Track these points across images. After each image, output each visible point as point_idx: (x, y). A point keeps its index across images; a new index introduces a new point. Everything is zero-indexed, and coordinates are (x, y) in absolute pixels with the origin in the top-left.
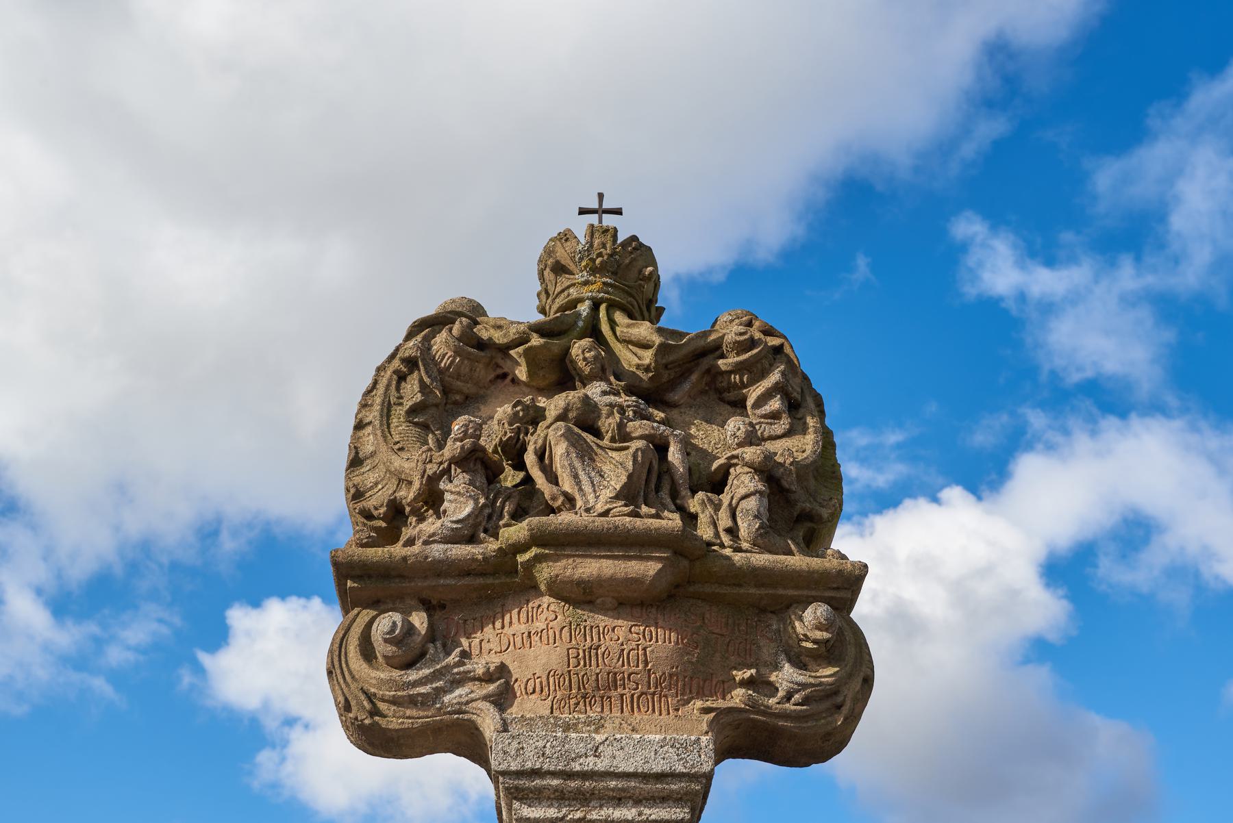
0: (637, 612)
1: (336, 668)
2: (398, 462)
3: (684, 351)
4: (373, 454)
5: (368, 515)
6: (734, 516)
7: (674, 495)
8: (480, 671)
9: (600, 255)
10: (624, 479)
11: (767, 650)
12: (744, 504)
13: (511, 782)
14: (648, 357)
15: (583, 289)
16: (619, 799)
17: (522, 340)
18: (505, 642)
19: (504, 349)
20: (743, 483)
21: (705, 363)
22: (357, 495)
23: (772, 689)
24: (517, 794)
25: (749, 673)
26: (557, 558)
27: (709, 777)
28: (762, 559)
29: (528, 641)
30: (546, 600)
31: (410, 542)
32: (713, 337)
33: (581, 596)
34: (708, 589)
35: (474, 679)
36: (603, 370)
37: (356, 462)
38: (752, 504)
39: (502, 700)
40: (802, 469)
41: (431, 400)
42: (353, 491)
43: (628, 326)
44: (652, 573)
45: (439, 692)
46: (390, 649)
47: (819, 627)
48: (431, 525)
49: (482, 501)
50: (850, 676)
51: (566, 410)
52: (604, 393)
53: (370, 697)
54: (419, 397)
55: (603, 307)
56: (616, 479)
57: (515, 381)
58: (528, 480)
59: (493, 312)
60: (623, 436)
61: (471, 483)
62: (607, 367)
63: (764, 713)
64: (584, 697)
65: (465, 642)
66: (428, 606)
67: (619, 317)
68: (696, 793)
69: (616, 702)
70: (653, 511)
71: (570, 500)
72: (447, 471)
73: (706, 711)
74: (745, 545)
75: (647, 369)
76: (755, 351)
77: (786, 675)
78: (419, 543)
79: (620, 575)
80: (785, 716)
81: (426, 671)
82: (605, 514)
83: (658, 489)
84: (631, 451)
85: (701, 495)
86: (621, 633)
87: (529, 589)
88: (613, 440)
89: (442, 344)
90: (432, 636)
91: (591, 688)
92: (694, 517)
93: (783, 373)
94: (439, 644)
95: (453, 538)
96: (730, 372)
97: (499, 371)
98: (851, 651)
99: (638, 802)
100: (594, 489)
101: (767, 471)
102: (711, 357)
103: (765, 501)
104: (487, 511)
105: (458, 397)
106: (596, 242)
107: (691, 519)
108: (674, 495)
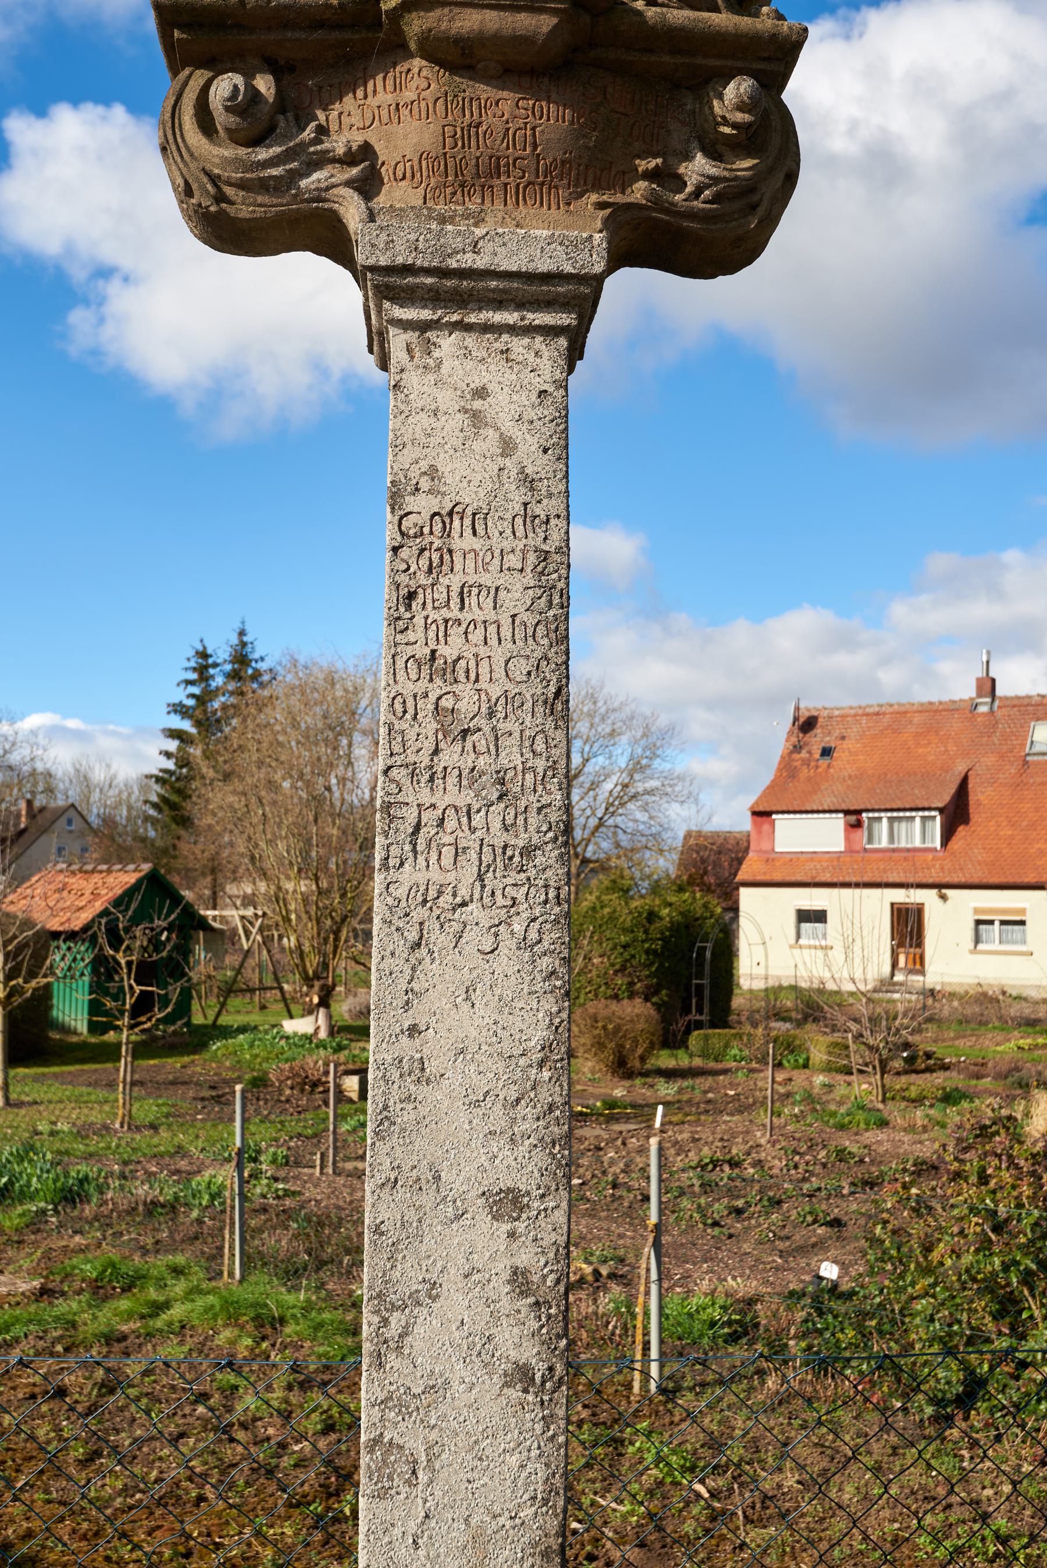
8: (340, 150)
13: (380, 279)
16: (499, 303)
18: (368, 115)
25: (653, 163)
27: (597, 282)
29: (395, 114)
30: (417, 63)
35: (335, 160)
39: (368, 186)
44: (545, 29)
46: (233, 120)
47: (741, 107)
50: (771, 170)
53: (214, 179)
63: (667, 212)
64: (462, 186)
65: (321, 115)
68: (585, 297)
69: (498, 192)
73: (601, 206)
77: (698, 167)
79: (507, 32)
80: (692, 215)
81: (278, 149)
86: (506, 107)
91: (470, 175)
94: (290, 116)
99: (520, 305)
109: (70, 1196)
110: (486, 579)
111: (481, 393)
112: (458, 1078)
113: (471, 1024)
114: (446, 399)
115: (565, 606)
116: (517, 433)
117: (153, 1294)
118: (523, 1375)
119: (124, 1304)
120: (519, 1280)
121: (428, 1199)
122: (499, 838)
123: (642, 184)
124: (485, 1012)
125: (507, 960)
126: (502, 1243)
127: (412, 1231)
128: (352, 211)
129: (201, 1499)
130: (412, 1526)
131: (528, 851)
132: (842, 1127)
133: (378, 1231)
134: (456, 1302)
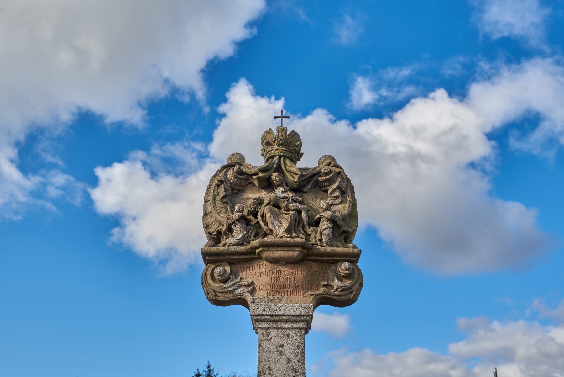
0: (292, 266)
2: (219, 218)
3: (308, 176)
4: (211, 212)
5: (210, 234)
6: (321, 235)
8: (246, 284)
9: (281, 140)
10: (287, 225)
12: (324, 232)
13: (255, 317)
14: (296, 177)
15: (276, 151)
16: (286, 321)
17: (256, 174)
18: (253, 275)
19: (251, 175)
20: (325, 224)
21: (315, 178)
22: (207, 227)
23: (332, 287)
24: (258, 321)
25: (326, 283)
26: (268, 250)
27: (312, 316)
28: (329, 249)
29: (259, 274)
30: (265, 262)
31: (224, 245)
32: (318, 169)
33: (275, 261)
34: (313, 258)
35: (244, 286)
36: (282, 183)
37: (205, 215)
38: (326, 232)
39: (252, 292)
40: (344, 218)
41: (228, 194)
42: (205, 225)
43: (290, 166)
44: (296, 255)
45: (234, 290)
46: (220, 278)
47: (346, 270)
48: (230, 240)
49: (245, 233)
50: (355, 283)
51: (270, 201)
52: (283, 192)
53: (214, 291)
54: (224, 194)
55: (282, 158)
56: (286, 225)
57: (254, 185)
58: (258, 222)
59: (247, 162)
60: (288, 210)
61: (241, 227)
63: (329, 295)
64: (276, 291)
65: (241, 275)
66: (230, 264)
67: (288, 162)
68: (308, 320)
69: (286, 293)
70: (296, 235)
71: (271, 231)
72: (234, 222)
73: (312, 295)
74: (324, 245)
75: (296, 182)
76: (331, 175)
77: (336, 283)
78: (227, 246)
79: (286, 256)
80: (336, 296)
81: (230, 284)
82: (282, 237)
83: (298, 226)
84: (290, 215)
85: (311, 228)
86: (287, 272)
87: (260, 258)
88: (284, 210)
89: (230, 174)
90: (231, 273)
91: (278, 288)
92: (309, 235)
93: (340, 182)
94: (234, 276)
95: (237, 244)
96: (323, 182)
97: (249, 181)
98: (356, 275)
99: (292, 322)
100: (279, 228)
101: (332, 220)
102: (317, 176)
103: (331, 230)
104: (247, 236)
105: (236, 191)
106: (280, 134)
107: (308, 236)
108: (304, 227)
111: (282, 346)
114: (273, 348)
116: (291, 357)
123: (322, 289)
128: (249, 298)
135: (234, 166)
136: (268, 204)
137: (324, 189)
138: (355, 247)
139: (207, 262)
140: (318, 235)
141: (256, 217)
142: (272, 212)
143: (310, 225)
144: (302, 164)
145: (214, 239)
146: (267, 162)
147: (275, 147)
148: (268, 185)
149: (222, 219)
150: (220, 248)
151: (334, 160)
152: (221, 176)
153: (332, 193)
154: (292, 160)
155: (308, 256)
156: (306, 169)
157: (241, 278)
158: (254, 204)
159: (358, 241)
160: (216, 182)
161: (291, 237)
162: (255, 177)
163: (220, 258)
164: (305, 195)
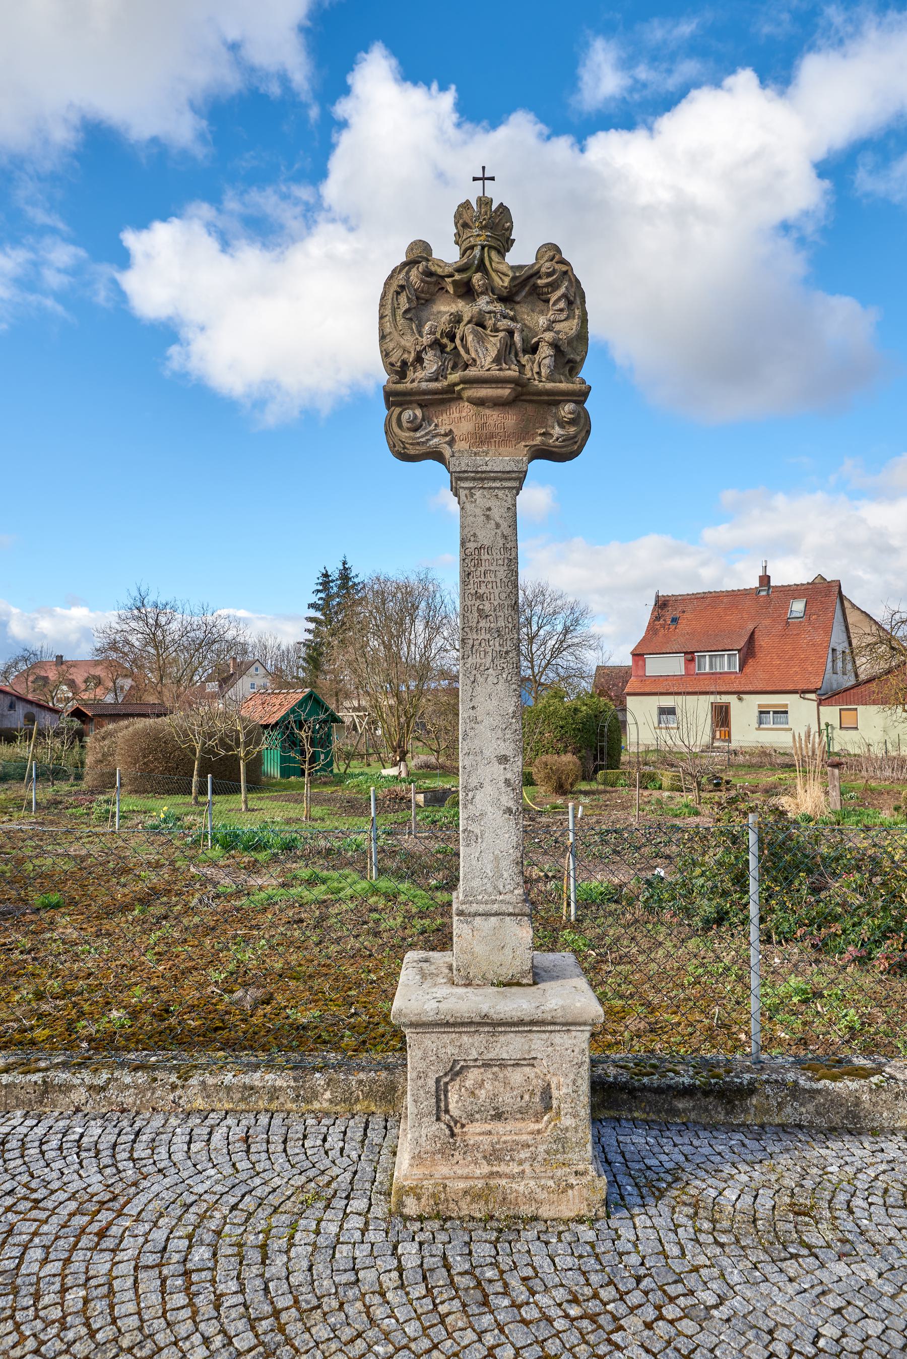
1: (388, 431)
2: (403, 343)
5: (392, 365)
7: (516, 355)
11: (550, 421)
14: (507, 281)
16: (494, 479)
17: (451, 276)
19: (443, 277)
20: (545, 351)
22: (386, 354)
24: (459, 479)
26: (470, 388)
27: (526, 472)
28: (550, 386)
29: (459, 420)
31: (413, 381)
33: (480, 403)
34: (528, 398)
37: (383, 337)
39: (451, 443)
40: (570, 342)
48: (420, 374)
53: (403, 442)
54: (407, 306)
56: (493, 353)
58: (456, 348)
59: (435, 255)
60: (496, 330)
62: (490, 288)
66: (421, 406)
67: (494, 254)
77: (557, 431)
82: (488, 370)
86: (495, 417)
87: (460, 398)
89: (415, 275)
90: (423, 419)
91: (483, 438)
98: (582, 421)
99: (501, 480)
100: (484, 356)
108: (516, 355)
109: (288, 847)
110: (492, 568)
111: (489, 509)
112: (487, 721)
113: (492, 705)
114: (478, 511)
115: (517, 576)
116: (501, 521)
117: (336, 884)
118: (509, 811)
119: (323, 888)
120: (507, 782)
121: (479, 758)
122: (498, 648)
123: (539, 438)
124: (495, 703)
125: (501, 686)
126: (502, 771)
127: (475, 767)
128: (447, 452)
129: (370, 956)
130: (477, 855)
131: (507, 653)
132: (676, 816)
133: (464, 768)
134: (488, 788)
135: (419, 262)
136: (469, 322)
137: (543, 297)
138: (584, 382)
139: (389, 405)
140: (536, 365)
141: (452, 339)
142: (475, 334)
143: (525, 352)
144: (514, 258)
145: (397, 373)
146: (463, 255)
147: (476, 231)
148: (467, 292)
149: (408, 344)
150: (407, 385)
151: (558, 251)
152: (401, 278)
153: (554, 304)
154: (499, 252)
155: (522, 395)
156: (520, 267)
157: (436, 425)
158: (450, 322)
159: (586, 373)
160: (394, 287)
161: (500, 370)
162: (448, 280)
163: (408, 398)
164: (517, 307)
